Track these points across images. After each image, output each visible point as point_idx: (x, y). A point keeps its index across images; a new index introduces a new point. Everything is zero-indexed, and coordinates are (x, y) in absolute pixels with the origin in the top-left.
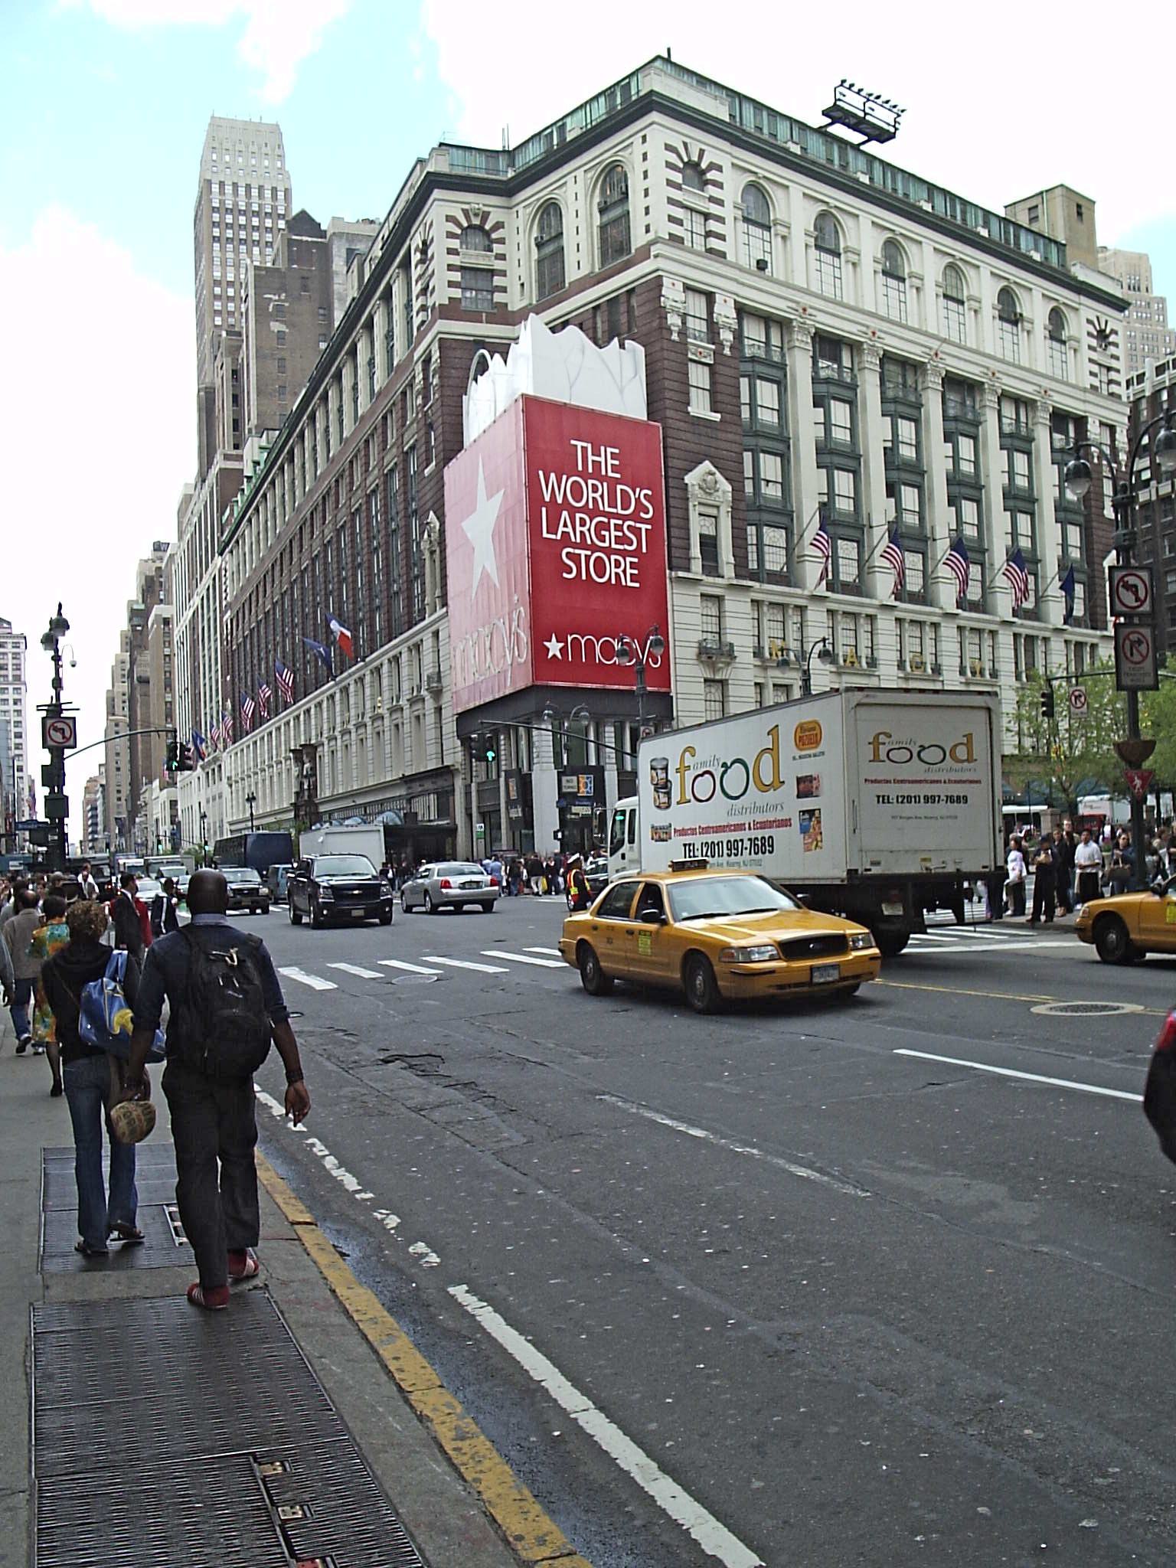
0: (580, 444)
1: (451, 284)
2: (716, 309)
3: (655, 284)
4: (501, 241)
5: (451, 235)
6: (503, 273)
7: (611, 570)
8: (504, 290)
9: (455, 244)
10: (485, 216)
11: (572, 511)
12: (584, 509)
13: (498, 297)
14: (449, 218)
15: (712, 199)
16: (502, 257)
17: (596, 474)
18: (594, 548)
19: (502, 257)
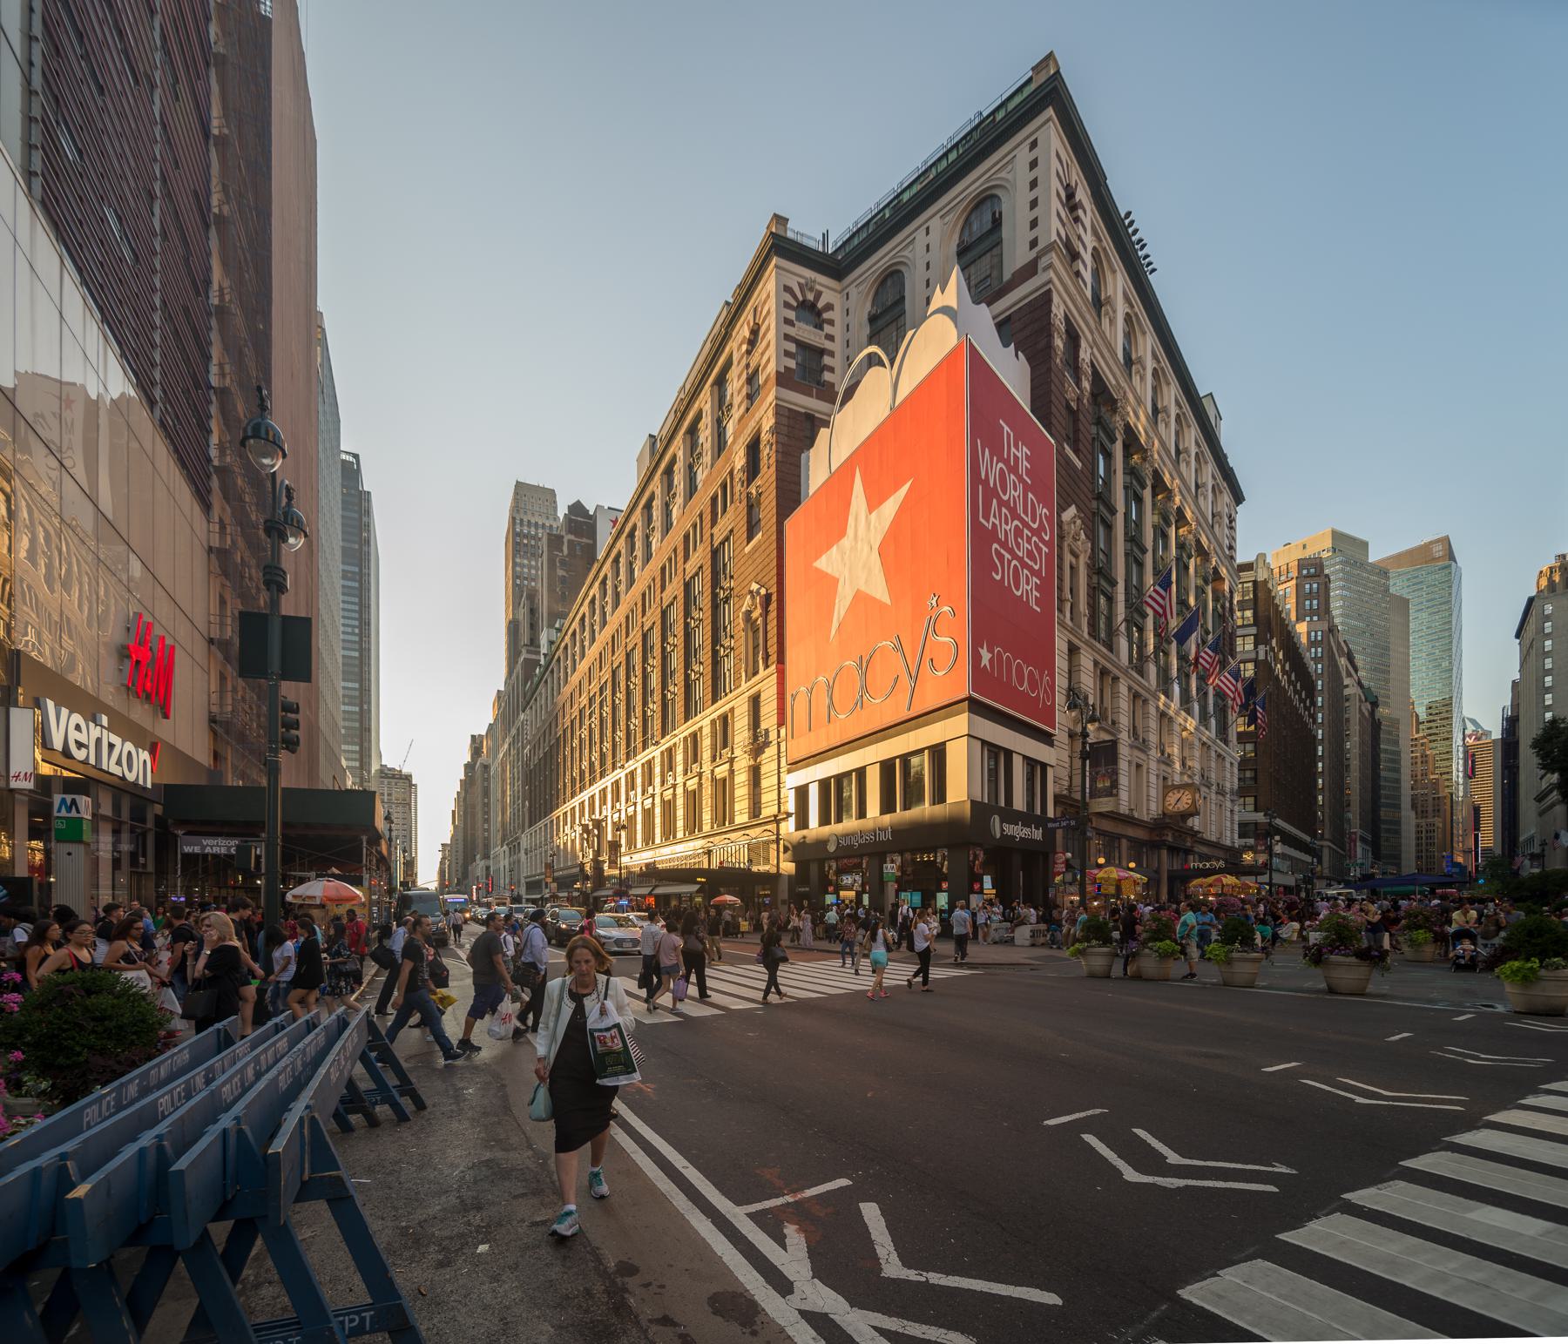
0: (1006, 428)
1: (787, 354)
2: (1082, 355)
3: (1045, 299)
4: (831, 322)
5: (787, 305)
6: (832, 354)
7: (1024, 586)
8: (832, 370)
9: (792, 315)
10: (818, 295)
11: (1001, 503)
12: (1005, 504)
13: (827, 376)
14: (787, 289)
15: (1079, 237)
16: (830, 338)
17: (1014, 470)
18: (1015, 557)
19: (830, 338)
